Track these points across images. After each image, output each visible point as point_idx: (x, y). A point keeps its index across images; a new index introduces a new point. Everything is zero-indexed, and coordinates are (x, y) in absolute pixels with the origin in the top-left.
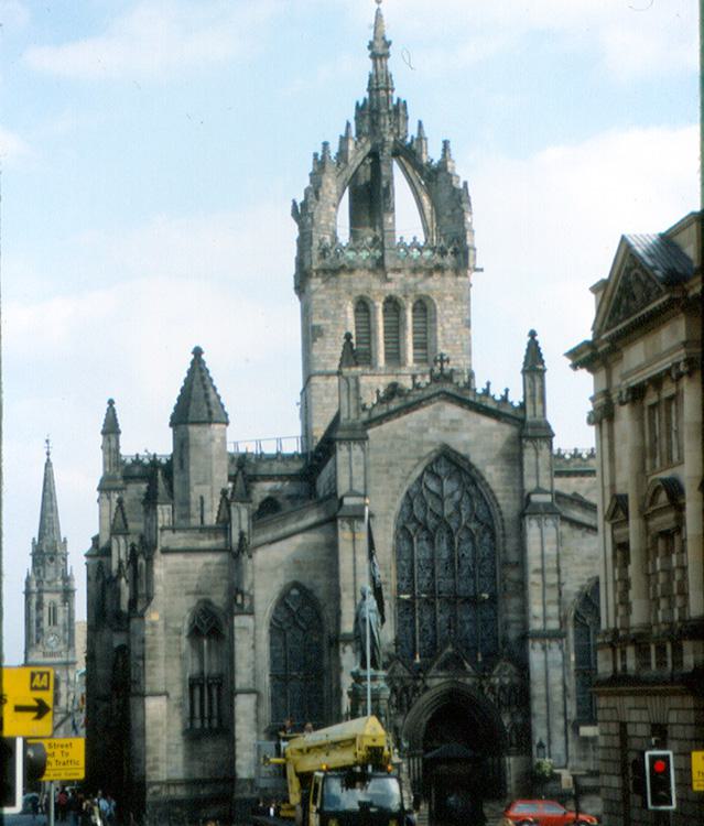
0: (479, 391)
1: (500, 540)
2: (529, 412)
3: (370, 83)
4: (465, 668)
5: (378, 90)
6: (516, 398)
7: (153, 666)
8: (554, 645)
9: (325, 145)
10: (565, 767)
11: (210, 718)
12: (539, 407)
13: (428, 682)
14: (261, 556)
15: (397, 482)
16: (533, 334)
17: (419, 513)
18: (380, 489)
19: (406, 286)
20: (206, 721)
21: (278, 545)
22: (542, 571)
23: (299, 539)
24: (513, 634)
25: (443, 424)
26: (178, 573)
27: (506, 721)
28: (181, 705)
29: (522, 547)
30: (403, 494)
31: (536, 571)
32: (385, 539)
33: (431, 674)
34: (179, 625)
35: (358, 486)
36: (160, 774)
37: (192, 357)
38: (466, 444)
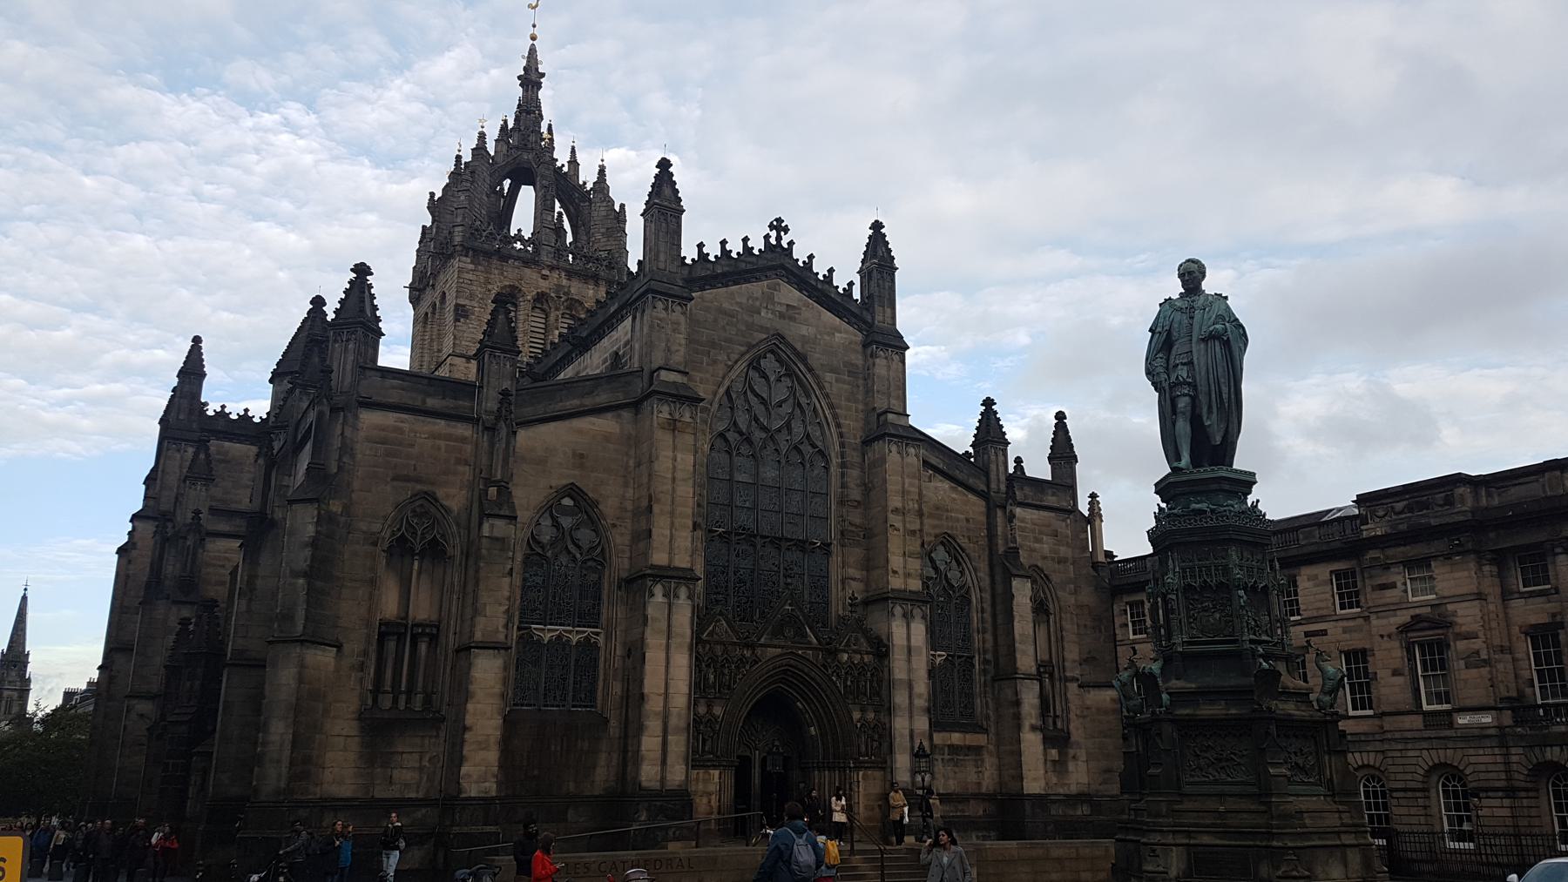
1: (834, 470)
2: (879, 317)
3: (519, 106)
4: (806, 636)
5: (528, 113)
6: (856, 294)
8: (917, 612)
9: (482, 136)
11: (410, 692)
12: (889, 311)
14: (523, 436)
15: (721, 371)
17: (743, 421)
18: (697, 375)
19: (559, 287)
20: (403, 698)
21: (552, 425)
23: (577, 423)
25: (778, 308)
26: (383, 442)
27: (856, 715)
28: (362, 667)
30: (722, 390)
33: (763, 640)
34: (376, 527)
35: (678, 358)
37: (311, 306)
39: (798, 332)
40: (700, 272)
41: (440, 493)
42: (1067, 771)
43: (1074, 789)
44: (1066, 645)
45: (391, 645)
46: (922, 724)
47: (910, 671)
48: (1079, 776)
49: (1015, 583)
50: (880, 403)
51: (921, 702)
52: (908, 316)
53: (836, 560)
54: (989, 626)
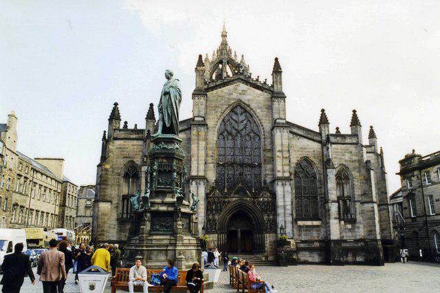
0: (255, 79)
1: (262, 140)
6: (270, 83)
7: (105, 188)
8: (287, 183)
10: (292, 239)
13: (230, 199)
15: (219, 114)
16: (276, 59)
18: (211, 117)
22: (281, 151)
24: (268, 180)
26: (121, 148)
27: (265, 217)
28: (117, 207)
29: (272, 143)
30: (221, 120)
31: (279, 151)
32: (213, 136)
34: (119, 171)
35: (202, 113)
36: (105, 237)
38: (249, 100)
39: (245, 99)
40: (211, 85)
41: (135, 160)
42: (355, 232)
43: (358, 238)
44: (355, 190)
45: (126, 202)
46: (289, 219)
47: (284, 201)
48: (361, 232)
49: (328, 170)
50: (276, 116)
51: (289, 212)
52: (286, 88)
53: (263, 169)
54: (323, 186)
